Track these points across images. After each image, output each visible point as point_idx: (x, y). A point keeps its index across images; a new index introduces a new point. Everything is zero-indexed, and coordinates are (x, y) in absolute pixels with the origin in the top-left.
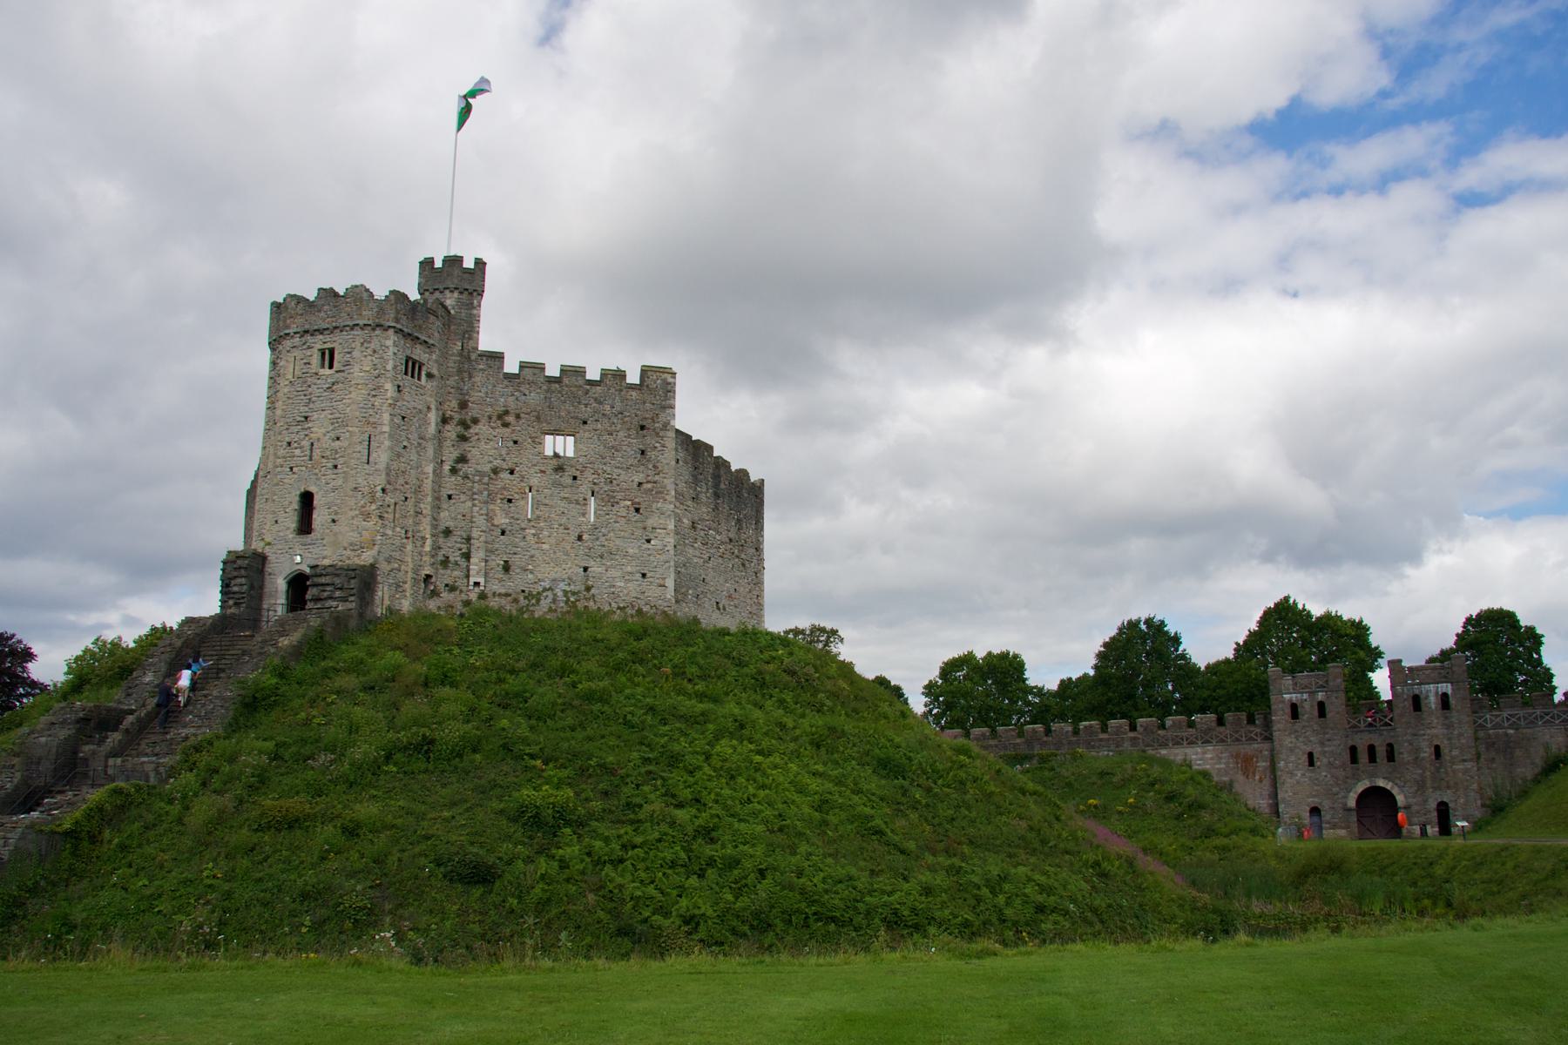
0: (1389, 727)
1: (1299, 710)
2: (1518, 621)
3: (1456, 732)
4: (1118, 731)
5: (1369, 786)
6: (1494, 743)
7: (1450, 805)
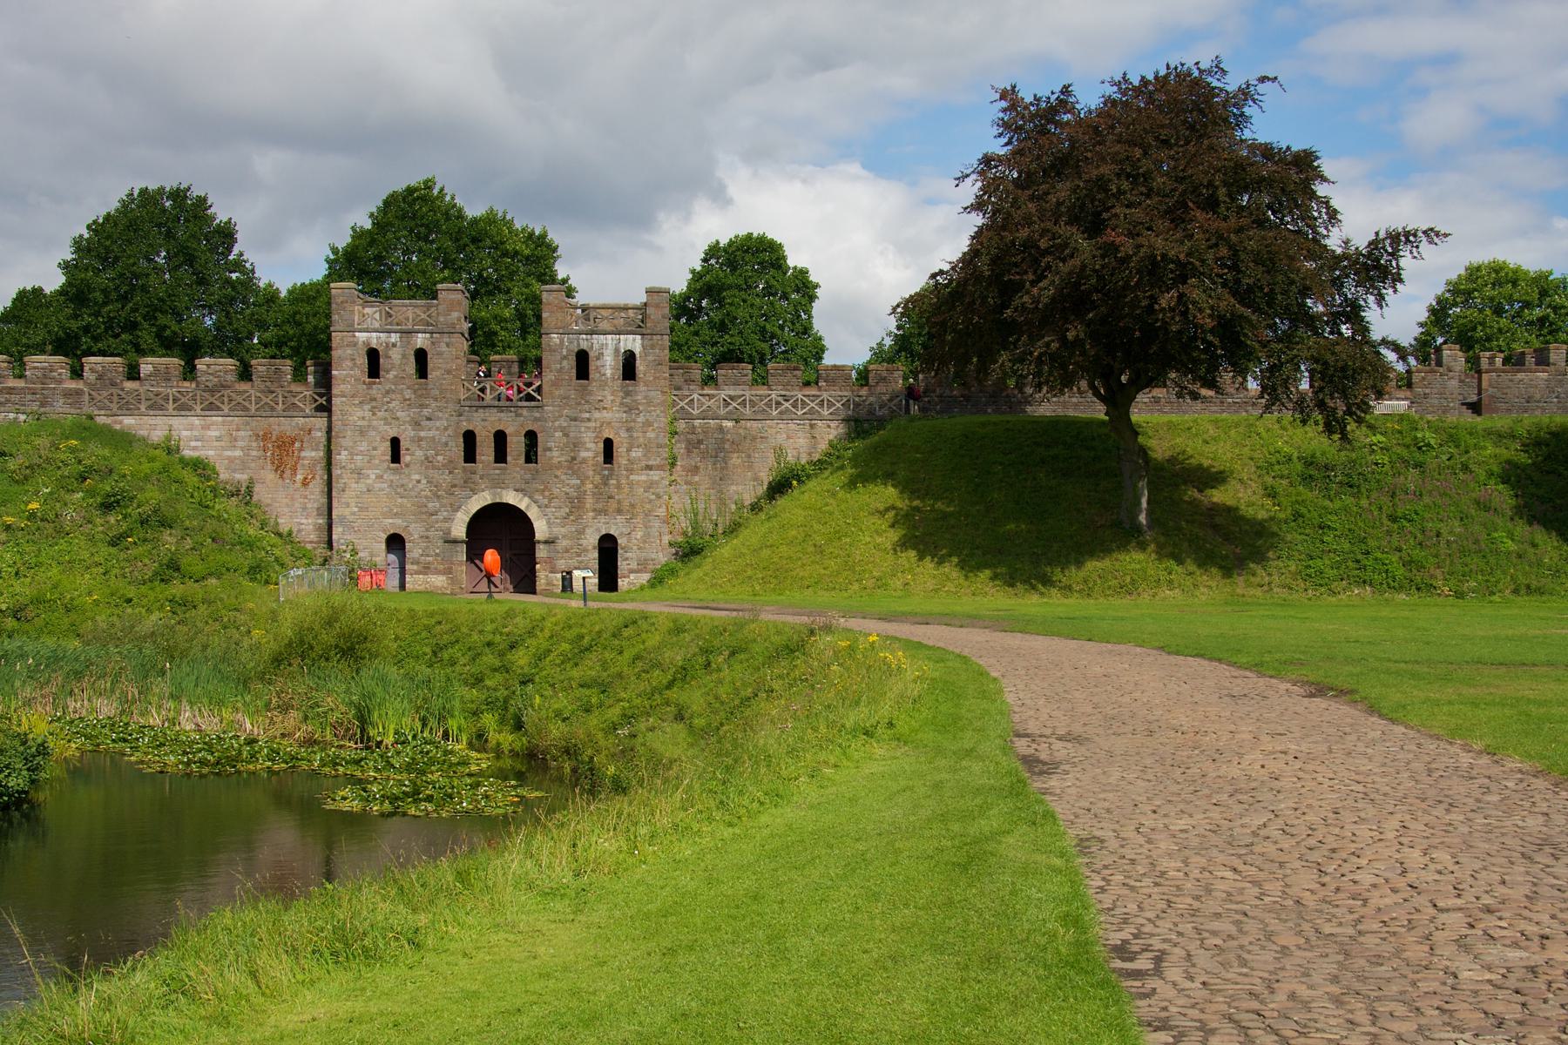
0: (533, 404)
1: (381, 360)
2: (784, 258)
3: (641, 419)
4: (46, 376)
5: (490, 502)
6: (700, 442)
7: (619, 541)
